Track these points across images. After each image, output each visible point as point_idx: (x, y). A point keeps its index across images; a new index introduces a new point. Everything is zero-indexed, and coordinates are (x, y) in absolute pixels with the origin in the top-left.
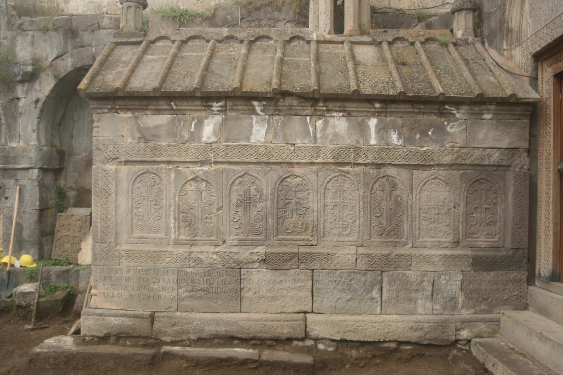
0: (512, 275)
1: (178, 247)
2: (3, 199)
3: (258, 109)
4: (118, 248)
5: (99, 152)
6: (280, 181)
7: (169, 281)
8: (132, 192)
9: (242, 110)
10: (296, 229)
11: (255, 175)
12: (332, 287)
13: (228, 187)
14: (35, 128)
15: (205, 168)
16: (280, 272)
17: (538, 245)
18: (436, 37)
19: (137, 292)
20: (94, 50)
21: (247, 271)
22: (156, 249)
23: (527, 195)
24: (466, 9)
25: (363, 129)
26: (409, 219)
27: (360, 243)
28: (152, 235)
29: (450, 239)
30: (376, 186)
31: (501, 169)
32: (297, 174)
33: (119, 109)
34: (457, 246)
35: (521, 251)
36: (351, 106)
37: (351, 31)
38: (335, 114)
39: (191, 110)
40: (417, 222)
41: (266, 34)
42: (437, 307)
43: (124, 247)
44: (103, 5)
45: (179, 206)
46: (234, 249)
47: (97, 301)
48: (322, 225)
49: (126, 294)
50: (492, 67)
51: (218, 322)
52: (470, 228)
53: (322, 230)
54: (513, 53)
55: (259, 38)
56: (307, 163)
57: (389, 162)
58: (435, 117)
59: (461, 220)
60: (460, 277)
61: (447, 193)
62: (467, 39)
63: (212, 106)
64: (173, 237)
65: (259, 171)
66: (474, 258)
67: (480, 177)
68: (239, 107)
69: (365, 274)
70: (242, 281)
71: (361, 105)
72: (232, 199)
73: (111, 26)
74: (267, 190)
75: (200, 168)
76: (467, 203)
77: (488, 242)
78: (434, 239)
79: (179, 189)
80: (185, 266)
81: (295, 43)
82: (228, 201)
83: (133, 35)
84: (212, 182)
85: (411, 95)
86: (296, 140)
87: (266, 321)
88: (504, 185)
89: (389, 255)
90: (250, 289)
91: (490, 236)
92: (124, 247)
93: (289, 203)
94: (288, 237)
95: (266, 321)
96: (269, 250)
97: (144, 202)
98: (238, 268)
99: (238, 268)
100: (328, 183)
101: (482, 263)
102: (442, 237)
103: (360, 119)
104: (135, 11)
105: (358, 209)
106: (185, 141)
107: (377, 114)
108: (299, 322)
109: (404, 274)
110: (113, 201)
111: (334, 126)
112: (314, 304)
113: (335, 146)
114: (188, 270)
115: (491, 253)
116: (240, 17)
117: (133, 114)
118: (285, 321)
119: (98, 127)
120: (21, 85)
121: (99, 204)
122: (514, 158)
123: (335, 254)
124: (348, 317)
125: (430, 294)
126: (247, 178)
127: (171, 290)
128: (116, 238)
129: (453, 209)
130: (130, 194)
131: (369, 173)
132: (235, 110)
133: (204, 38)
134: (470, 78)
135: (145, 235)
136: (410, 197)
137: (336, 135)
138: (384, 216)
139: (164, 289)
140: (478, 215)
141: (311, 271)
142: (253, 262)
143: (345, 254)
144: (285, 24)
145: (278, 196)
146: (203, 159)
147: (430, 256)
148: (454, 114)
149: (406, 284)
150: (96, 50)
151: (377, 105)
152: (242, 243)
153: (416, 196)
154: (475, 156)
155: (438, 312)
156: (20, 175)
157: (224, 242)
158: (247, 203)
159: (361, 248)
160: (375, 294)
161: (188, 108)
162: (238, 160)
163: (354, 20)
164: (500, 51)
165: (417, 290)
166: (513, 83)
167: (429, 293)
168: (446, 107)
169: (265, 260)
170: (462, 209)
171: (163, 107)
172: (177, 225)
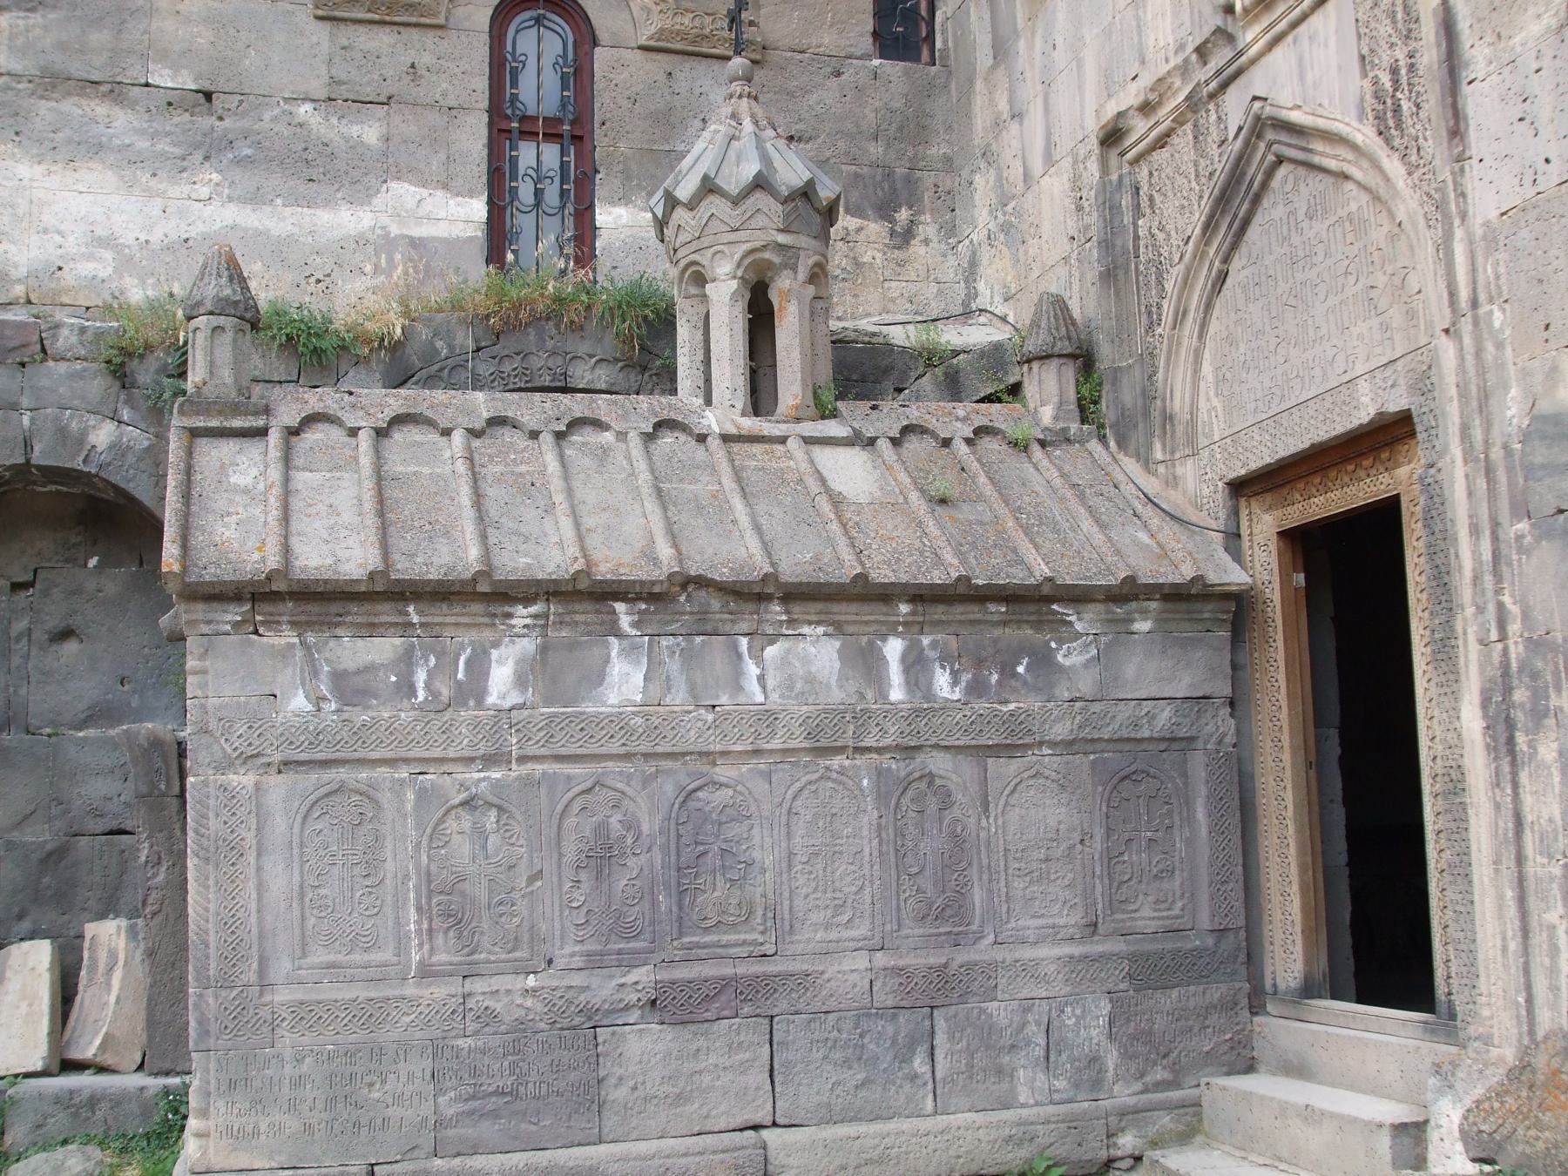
0: (1217, 992)
1: (430, 985)
3: (625, 622)
4: (267, 998)
5: (205, 739)
6: (681, 799)
7: (411, 1077)
8: (302, 845)
9: (586, 623)
10: (724, 918)
11: (620, 786)
12: (820, 1055)
13: (555, 821)
15: (496, 775)
16: (692, 1027)
17: (1266, 918)
18: (996, 425)
20: (26, 420)
21: (613, 1034)
22: (373, 994)
23: (1237, 803)
24: (1060, 356)
25: (867, 663)
26: (985, 877)
27: (877, 941)
28: (357, 957)
29: (1076, 917)
30: (905, 801)
31: (1175, 746)
32: (723, 780)
33: (263, 623)
34: (1094, 933)
35: (1231, 935)
37: (797, 407)
38: (806, 630)
39: (457, 624)
40: (1003, 883)
41: (588, 414)
42: (1060, 1084)
43: (282, 995)
44: (14, 274)
45: (429, 874)
46: (577, 980)
47: (211, 1150)
48: (786, 903)
49: (292, 1124)
50: (1139, 508)
52: (1119, 888)
53: (787, 916)
54: (1179, 470)
55: (576, 424)
56: (747, 752)
57: (934, 741)
58: (1030, 632)
59: (1098, 873)
60: (1105, 1007)
61: (1063, 810)
62: (1065, 430)
63: (510, 616)
64: (415, 957)
65: (630, 777)
66: (1133, 958)
67: (1133, 768)
68: (578, 618)
69: (894, 1016)
70: (601, 1060)
71: (866, 608)
72: (565, 850)
74: (649, 824)
75: (482, 775)
76: (1109, 831)
77: (1159, 918)
79: (429, 831)
80: (453, 1033)
81: (667, 440)
82: (555, 856)
83: (236, 409)
84: (511, 808)
85: (980, 582)
86: (717, 697)
87: (668, 1157)
88: (1186, 784)
89: (946, 966)
90: (621, 1079)
91: (1162, 906)
92: (282, 995)
93: (705, 853)
94: (707, 939)
95: (668, 1157)
96: (664, 975)
97: (336, 871)
98: (588, 1026)
99: (588, 1026)
100: (794, 798)
101: (1152, 970)
102: (1060, 914)
103: (865, 639)
104: (235, 340)
105: (867, 858)
106: (441, 707)
107: (901, 629)
108: (749, 1151)
109: (983, 1011)
110: (252, 870)
111: (806, 660)
112: (778, 1104)
113: (811, 708)
114: (460, 1042)
115: (1169, 946)
116: (471, 345)
117: (299, 636)
118: (714, 1152)
119: (204, 672)
121: (211, 882)
122: (1203, 721)
123: (822, 973)
124: (863, 1128)
125: (1042, 1053)
126: (601, 795)
127: (416, 1100)
128: (262, 972)
129: (1079, 847)
130: (296, 850)
131: (889, 769)
132: (569, 624)
133: (430, 423)
134: (1098, 538)
135: (340, 957)
136: (984, 823)
137: (810, 679)
138: (927, 873)
139: (398, 1099)
140: (1135, 858)
141: (767, 1021)
142: (628, 1008)
143: (844, 973)
144: (593, 368)
145: (679, 836)
146: (491, 750)
147: (1037, 963)
148: (1070, 622)
149: (986, 1034)
150: (32, 421)
151: (904, 608)
152: (595, 962)
153: (996, 819)
154: (1119, 718)
155: (1065, 1096)
157: (550, 962)
158: (602, 857)
159: (879, 954)
160: (919, 1064)
161: (448, 620)
162: (579, 751)
163: (803, 379)
164: (1147, 463)
165: (1013, 1046)
166: (1190, 546)
167: (1040, 1052)
168: (1055, 607)
169: (654, 1001)
170: (1098, 845)
171: (384, 619)
172: (425, 926)
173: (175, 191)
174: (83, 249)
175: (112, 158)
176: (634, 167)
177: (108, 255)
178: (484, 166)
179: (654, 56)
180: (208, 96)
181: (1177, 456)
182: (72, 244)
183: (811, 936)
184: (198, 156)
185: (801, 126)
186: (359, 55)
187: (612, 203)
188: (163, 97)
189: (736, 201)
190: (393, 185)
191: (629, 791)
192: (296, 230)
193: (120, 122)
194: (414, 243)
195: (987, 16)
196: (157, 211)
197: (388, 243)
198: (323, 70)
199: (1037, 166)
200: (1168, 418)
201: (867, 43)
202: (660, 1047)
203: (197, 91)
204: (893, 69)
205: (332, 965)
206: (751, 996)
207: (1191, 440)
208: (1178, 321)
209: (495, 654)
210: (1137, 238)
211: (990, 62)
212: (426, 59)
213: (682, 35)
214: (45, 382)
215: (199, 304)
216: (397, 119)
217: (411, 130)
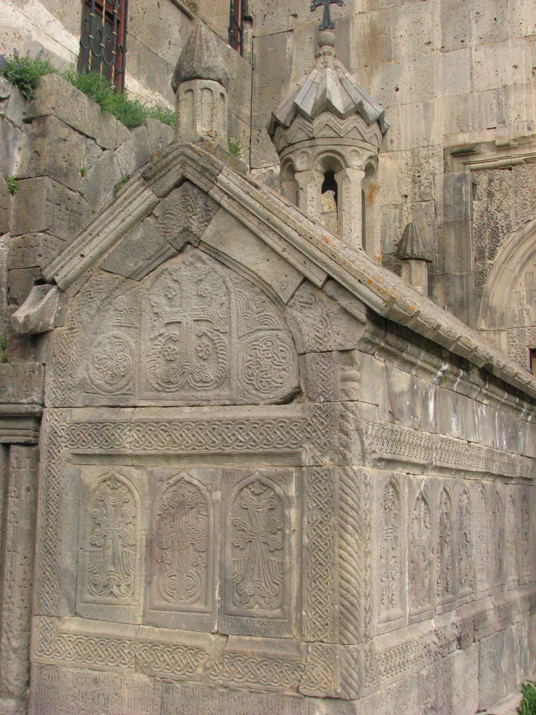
178: (80, 15)
181: (492, 329)
200: (489, 309)
207: (502, 323)
208: (509, 258)
210: (472, 209)
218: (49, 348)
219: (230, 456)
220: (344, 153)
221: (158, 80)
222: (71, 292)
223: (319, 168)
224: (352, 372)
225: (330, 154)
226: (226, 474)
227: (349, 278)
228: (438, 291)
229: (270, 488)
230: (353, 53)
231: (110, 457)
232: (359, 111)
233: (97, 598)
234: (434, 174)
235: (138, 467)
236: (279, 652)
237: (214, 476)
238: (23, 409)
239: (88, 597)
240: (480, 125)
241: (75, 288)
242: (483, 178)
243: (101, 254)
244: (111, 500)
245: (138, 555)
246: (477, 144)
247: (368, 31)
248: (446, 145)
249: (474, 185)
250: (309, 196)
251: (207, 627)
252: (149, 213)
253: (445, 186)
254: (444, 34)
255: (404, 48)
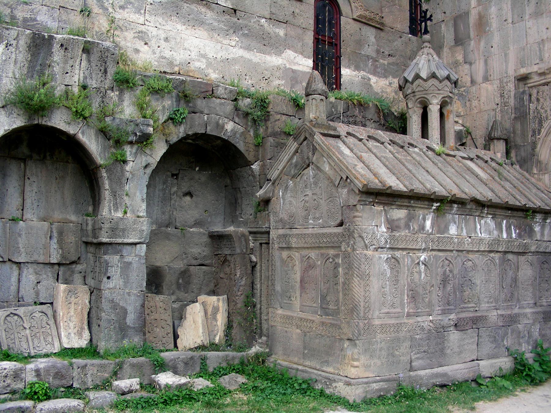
1: (409, 319)
2: (105, 279)
7: (406, 347)
14: (145, 197)
16: (464, 332)
19: (386, 360)
20: (206, 117)
22: (398, 322)
29: (532, 302)
36: (499, 212)
43: (377, 322)
46: (440, 318)
49: (379, 362)
51: (437, 375)
64: (406, 310)
66: (544, 313)
71: (503, 211)
73: (225, 97)
78: (526, 302)
94: (466, 306)
103: (499, 220)
114: (416, 336)
120: (129, 146)
128: (372, 315)
152: (444, 312)
156: (126, 250)
158: (445, 281)
159: (498, 311)
161: (419, 206)
167: (527, 338)
171: (405, 204)
173: (225, 42)
174: (197, 57)
175: (206, 27)
176: (351, 57)
177: (204, 61)
178: (312, 49)
179: (356, 22)
180: (235, 11)
181: (541, 172)
182: (194, 55)
183: (484, 306)
184: (232, 31)
185: (392, 52)
186: (279, 6)
187: (346, 68)
188: (223, 9)
189: (441, 82)
190: (288, 51)
191: (452, 261)
192: (260, 61)
193: (209, 15)
194: (293, 71)
195: (452, 30)
196: (219, 48)
197: (286, 70)
198: (268, 9)
199: (479, 78)
200: (539, 162)
201: (407, 30)
202: (457, 337)
203: (232, 9)
204: (414, 38)
205: (388, 313)
206: (476, 322)
207: (546, 169)
209: (427, 217)
210: (529, 109)
211: (453, 43)
212: (297, 11)
213: (365, 17)
214: (212, 105)
215: (314, 91)
216: (289, 29)
217: (293, 33)
218: (271, 206)
219: (322, 247)
220: (428, 98)
221: (362, 65)
222: (276, 184)
223: (419, 106)
224: (357, 214)
225: (422, 99)
226: (322, 255)
227: (352, 177)
228: (513, 154)
229: (334, 260)
230: (471, 29)
231: (289, 248)
232: (433, 76)
233: (287, 301)
234: (510, 91)
235: (297, 252)
236: (336, 322)
237: (318, 255)
238: (264, 230)
239: (285, 301)
240: (531, 62)
241: (277, 182)
242: (534, 91)
243: (284, 168)
244: (290, 265)
245: (298, 285)
246: (529, 73)
247: (477, 17)
248: (515, 75)
249: (530, 96)
250: (414, 120)
251: (316, 313)
252: (296, 152)
253: (515, 98)
254: (513, 15)
255: (494, 24)
